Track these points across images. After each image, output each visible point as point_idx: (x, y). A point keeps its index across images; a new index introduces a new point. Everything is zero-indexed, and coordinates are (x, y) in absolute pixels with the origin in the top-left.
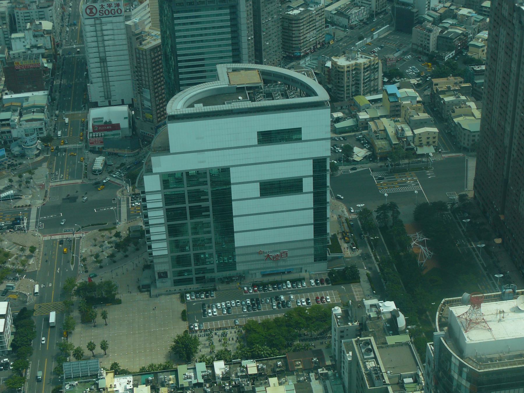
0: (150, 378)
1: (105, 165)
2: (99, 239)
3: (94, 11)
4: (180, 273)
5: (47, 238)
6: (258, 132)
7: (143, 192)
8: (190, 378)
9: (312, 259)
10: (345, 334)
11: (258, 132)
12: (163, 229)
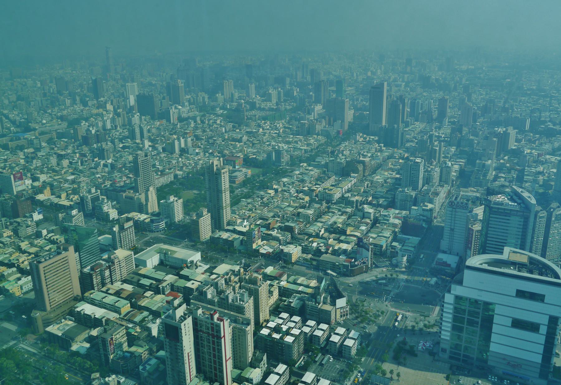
1: (436, 283)
2: (418, 320)
3: (453, 204)
5: (393, 310)
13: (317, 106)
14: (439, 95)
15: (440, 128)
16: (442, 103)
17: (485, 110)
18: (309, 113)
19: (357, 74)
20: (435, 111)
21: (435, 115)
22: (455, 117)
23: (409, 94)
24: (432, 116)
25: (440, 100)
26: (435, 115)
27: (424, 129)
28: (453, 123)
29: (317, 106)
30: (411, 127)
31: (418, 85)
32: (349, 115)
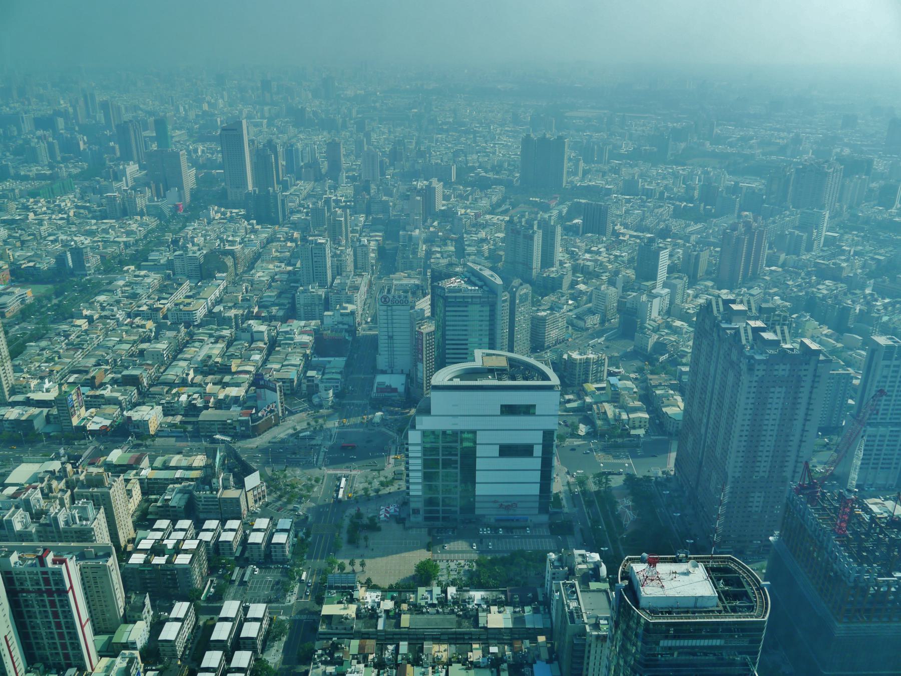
0: (395, 595)
3: (387, 300)
4: (430, 512)
6: (502, 406)
7: (407, 444)
8: (427, 599)
9: (537, 512)
10: (556, 576)
11: (502, 406)
12: (420, 474)
13: (128, 165)
14: (322, 138)
15: (335, 188)
16: (333, 148)
17: (395, 156)
18: (117, 177)
19: (184, 108)
20: (323, 162)
21: (325, 167)
22: (354, 170)
23: (278, 138)
24: (320, 170)
25: (328, 144)
26: (325, 167)
27: (312, 191)
28: (353, 179)
29: (128, 165)
30: (292, 190)
31: (287, 122)
32: (190, 177)
